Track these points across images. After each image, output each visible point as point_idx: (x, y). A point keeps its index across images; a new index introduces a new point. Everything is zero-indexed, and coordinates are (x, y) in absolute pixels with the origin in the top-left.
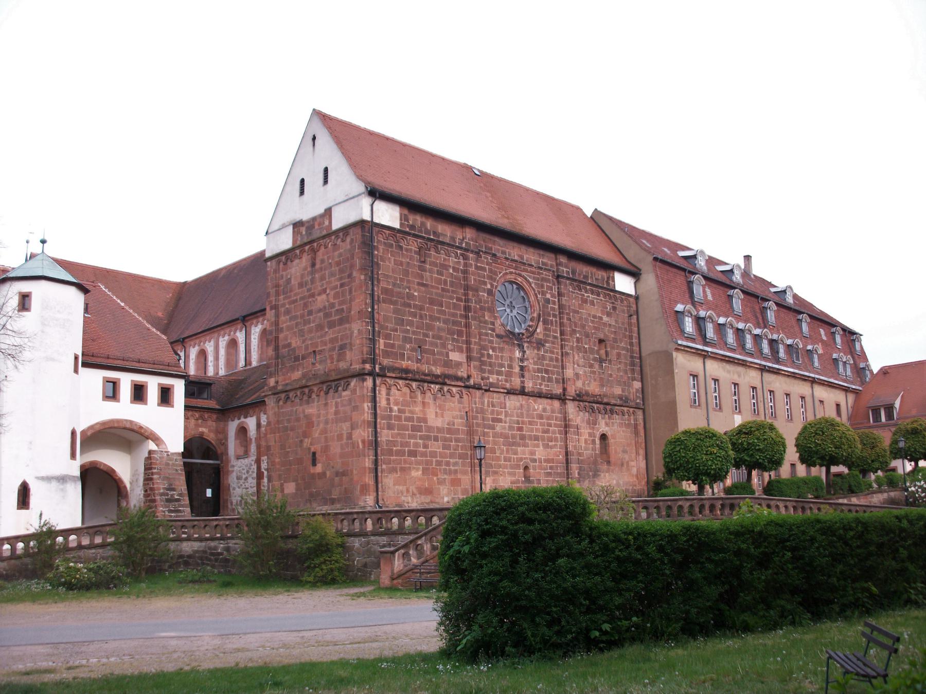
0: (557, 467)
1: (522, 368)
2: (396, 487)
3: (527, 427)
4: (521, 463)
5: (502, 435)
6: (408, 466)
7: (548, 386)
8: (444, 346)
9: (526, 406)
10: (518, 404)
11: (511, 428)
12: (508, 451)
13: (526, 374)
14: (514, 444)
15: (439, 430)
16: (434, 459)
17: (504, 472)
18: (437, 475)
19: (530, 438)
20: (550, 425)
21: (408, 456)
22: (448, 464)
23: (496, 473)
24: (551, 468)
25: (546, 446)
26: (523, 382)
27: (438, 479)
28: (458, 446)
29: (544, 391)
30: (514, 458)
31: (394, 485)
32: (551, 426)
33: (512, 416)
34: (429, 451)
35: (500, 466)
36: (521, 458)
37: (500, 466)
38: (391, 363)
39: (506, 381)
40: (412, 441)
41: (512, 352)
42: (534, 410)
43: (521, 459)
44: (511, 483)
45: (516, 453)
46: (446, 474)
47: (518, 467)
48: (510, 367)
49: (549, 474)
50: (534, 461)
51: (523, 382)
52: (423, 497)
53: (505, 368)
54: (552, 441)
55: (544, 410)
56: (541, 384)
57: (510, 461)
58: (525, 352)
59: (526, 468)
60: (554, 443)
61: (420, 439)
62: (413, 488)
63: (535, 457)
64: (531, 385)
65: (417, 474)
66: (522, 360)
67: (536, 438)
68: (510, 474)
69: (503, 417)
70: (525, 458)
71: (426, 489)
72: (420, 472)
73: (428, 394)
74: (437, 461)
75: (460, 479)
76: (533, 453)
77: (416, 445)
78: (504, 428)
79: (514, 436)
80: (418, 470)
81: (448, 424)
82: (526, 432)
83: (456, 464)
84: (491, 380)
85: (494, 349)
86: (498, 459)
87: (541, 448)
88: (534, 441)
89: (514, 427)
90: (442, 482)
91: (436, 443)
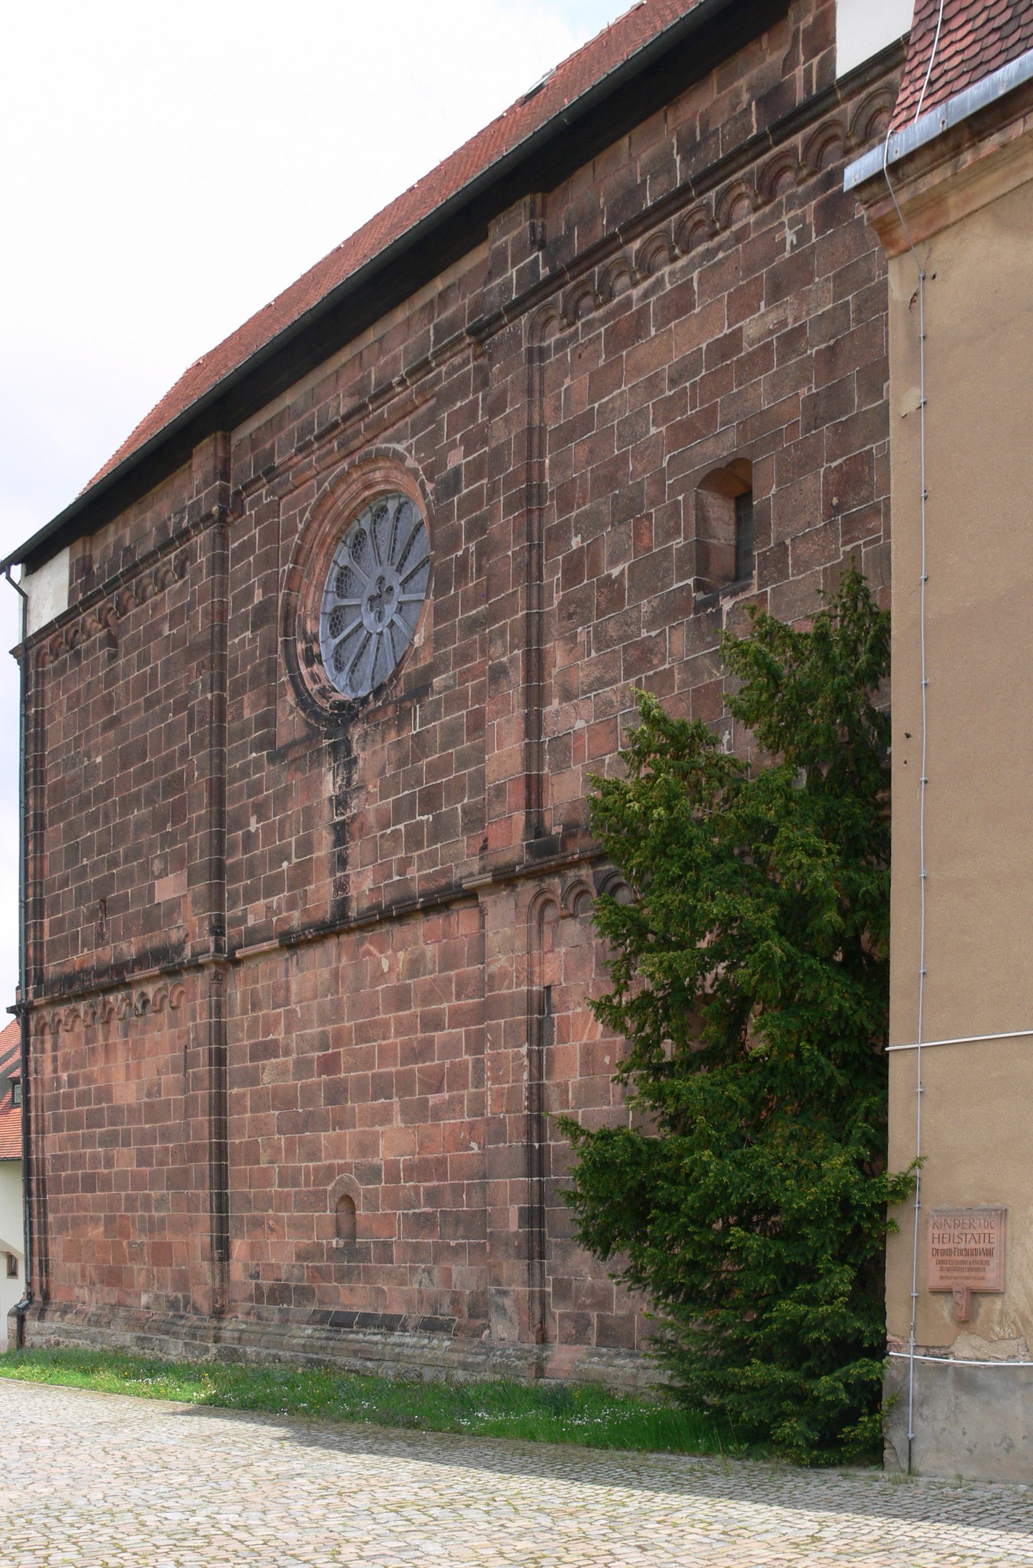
0: (457, 1190)
1: (341, 833)
2: (68, 1264)
3: (351, 1053)
4: (329, 1188)
5: (284, 1100)
6: (83, 1213)
7: (431, 859)
8: (146, 870)
9: (350, 973)
10: (325, 974)
11: (302, 1067)
12: (290, 1150)
13: (355, 849)
14: (311, 1122)
15: (133, 1112)
16: (123, 1193)
17: (278, 1220)
18: (128, 1237)
19: (361, 1095)
20: (433, 1023)
21: (83, 1191)
22: (147, 1205)
23: (257, 1223)
24: (433, 1196)
25: (417, 1112)
26: (341, 886)
27: (130, 1244)
28: (166, 1149)
29: (416, 887)
30: (307, 1168)
31: (66, 1259)
32: (438, 1026)
33: (306, 1024)
34: (116, 1173)
35: (268, 1202)
36: (330, 1168)
37: (268, 1202)
38: (58, 969)
39: (291, 904)
40: (88, 1151)
41: (312, 787)
42: (379, 976)
43: (329, 1173)
44: (299, 1257)
45: (313, 1156)
46: (142, 1230)
47: (317, 1200)
48: (306, 845)
49: (423, 1222)
50: (372, 1174)
51: (341, 886)
52: (106, 1289)
53: (288, 859)
54: (439, 1090)
55: (415, 967)
56: (405, 864)
57: (295, 1183)
58: (355, 761)
59: (347, 1201)
60: (446, 1095)
61: (100, 1146)
62: (90, 1269)
63: (376, 1161)
64: (368, 884)
65: (96, 1232)
66: (340, 802)
67: (382, 1087)
68: (295, 1225)
69: (279, 1035)
70: (342, 1169)
71: (111, 1270)
72: (102, 1229)
73: (116, 1024)
74: (128, 1197)
75: (170, 1244)
76: (367, 1147)
77: (95, 1157)
78: (282, 1072)
79: (309, 1095)
80: (96, 1221)
81: (149, 1095)
82: (348, 1070)
83: (162, 1202)
84: (251, 921)
85: (260, 811)
86: (265, 1178)
87: (398, 1121)
88: (374, 1099)
89: (309, 1062)
90: (135, 1255)
91: (125, 1150)
